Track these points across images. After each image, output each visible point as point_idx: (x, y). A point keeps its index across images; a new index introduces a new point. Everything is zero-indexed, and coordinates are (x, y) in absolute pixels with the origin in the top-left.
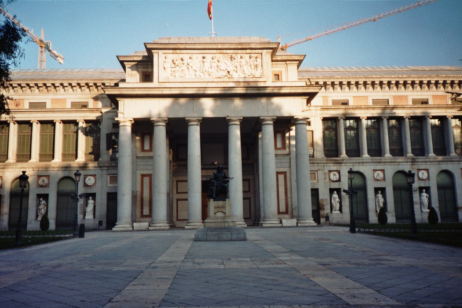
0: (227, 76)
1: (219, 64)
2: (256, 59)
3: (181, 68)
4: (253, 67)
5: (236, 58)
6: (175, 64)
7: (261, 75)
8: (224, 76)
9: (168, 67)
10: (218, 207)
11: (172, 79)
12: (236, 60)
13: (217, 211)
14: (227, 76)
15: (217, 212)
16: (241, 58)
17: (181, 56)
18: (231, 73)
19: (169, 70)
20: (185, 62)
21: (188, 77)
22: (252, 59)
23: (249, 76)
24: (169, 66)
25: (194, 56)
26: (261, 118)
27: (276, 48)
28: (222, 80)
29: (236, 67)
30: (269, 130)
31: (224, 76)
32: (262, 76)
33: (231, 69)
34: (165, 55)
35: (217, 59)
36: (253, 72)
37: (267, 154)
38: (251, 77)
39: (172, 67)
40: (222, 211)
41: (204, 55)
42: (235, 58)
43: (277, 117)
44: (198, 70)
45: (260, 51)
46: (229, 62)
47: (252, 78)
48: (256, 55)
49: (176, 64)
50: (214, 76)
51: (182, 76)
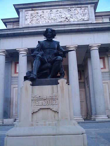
1: (61, 14)
7: (88, 19)
9: (28, 18)
10: (40, 99)
11: (31, 25)
12: (71, 12)
13: (39, 107)
15: (39, 110)
18: (68, 19)
21: (41, 23)
22: (82, 10)
25: (45, 11)
27: (97, 2)
28: (63, 23)
30: (95, 54)
33: (68, 16)
34: (26, 12)
35: (59, 11)
36: (83, 18)
38: (82, 20)
40: (51, 107)
41: (51, 10)
42: (71, 10)
43: (101, 44)
44: (47, 18)
45: (86, 5)
46: (67, 13)
48: (84, 8)
50: (57, 21)
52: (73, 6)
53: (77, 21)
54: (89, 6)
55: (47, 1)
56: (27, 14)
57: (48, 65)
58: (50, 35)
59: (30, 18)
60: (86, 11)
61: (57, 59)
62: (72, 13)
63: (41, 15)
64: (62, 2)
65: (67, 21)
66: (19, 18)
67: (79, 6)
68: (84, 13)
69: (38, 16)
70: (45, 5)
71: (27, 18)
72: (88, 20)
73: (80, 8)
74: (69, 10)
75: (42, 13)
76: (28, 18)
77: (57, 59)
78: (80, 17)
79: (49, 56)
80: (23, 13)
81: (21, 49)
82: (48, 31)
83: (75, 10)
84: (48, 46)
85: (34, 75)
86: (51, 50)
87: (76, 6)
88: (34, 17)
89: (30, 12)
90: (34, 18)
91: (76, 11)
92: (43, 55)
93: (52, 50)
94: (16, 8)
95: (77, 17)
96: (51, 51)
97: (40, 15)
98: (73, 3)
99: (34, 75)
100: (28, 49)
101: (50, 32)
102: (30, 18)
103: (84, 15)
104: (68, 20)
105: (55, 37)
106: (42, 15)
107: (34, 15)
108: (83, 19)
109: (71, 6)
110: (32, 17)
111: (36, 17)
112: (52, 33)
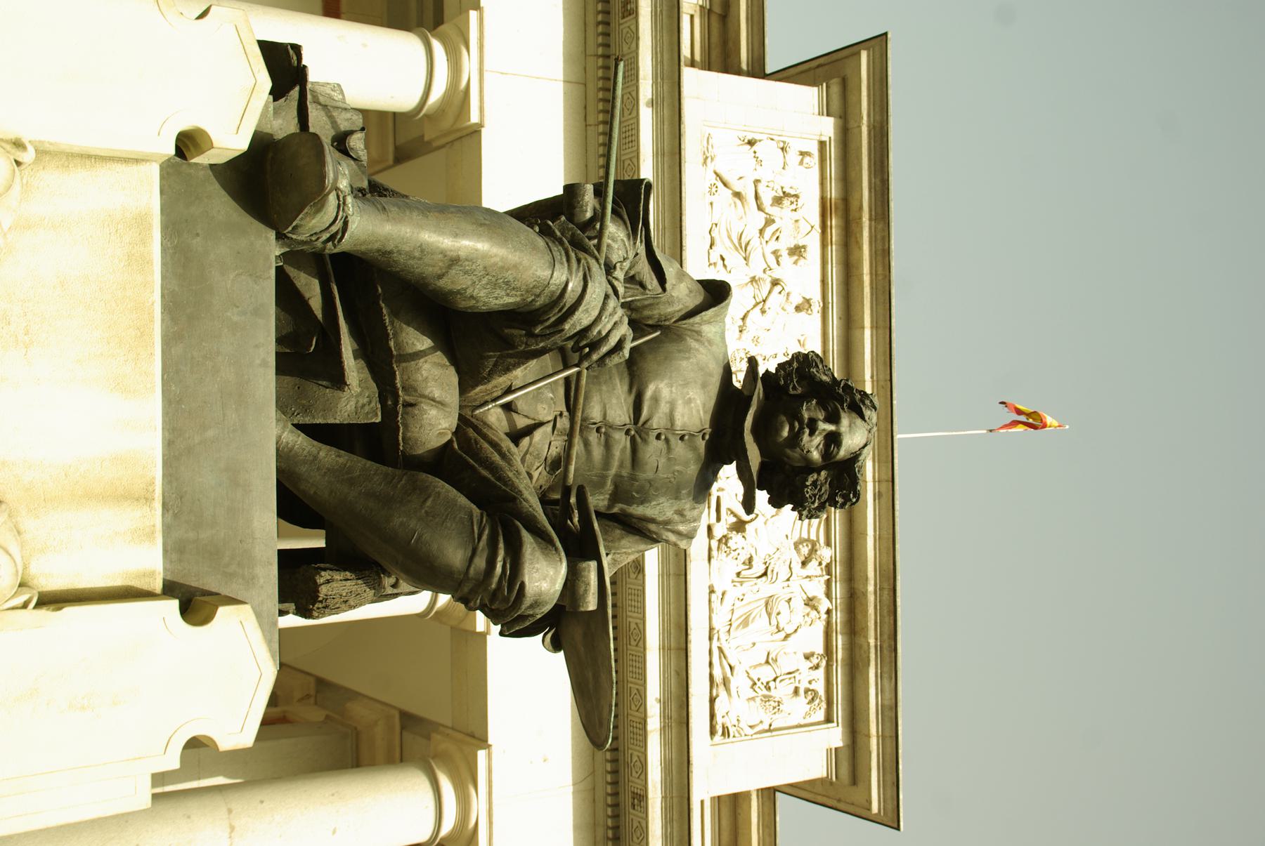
0: (718, 519)
2: (802, 692)
3: (755, 242)
4: (766, 674)
5: (813, 567)
6: (778, 201)
7: (726, 732)
8: (718, 498)
14: (718, 519)
16: (810, 602)
17: (813, 243)
18: (736, 539)
19: (738, 165)
20: (787, 270)
23: (720, 649)
24: (764, 174)
26: (482, 754)
27: (869, 809)
29: (765, 574)
31: (718, 498)
32: (718, 738)
34: (814, 149)
36: (739, 682)
37: (232, 828)
39: (761, 188)
42: (814, 563)
45: (839, 711)
47: (711, 676)
48: (820, 687)
49: (774, 211)
51: (717, 241)
52: (838, 590)
53: (715, 624)
54: (835, 736)
55: (894, 345)
56: (793, 157)
57: (440, 404)
58: (795, 438)
59: (757, 182)
60: (797, 709)
61: (527, 537)
62: (784, 574)
63: (775, 283)
64: (886, 487)
65: (720, 530)
66: (765, 76)
67: (839, 641)
68: (782, 691)
69: (772, 260)
70: (867, 333)
71: (766, 149)
72: (713, 732)
73: (820, 649)
74: (805, 550)
75: (796, 300)
76: (759, 162)
77: (527, 537)
78: (745, 650)
79: (541, 424)
80: (802, 115)
81: (469, 65)
82: (845, 421)
83: (810, 602)
84: (671, 418)
85: (341, 205)
86: (621, 442)
87: (838, 618)
88: (769, 222)
89: (808, 185)
90: (760, 219)
91: (798, 619)
92: (595, 345)
93: (617, 453)
94: (859, 54)
95: (745, 623)
96: (608, 446)
97: (777, 273)
98: (871, 588)
99: (341, 205)
100: (475, 132)
101: (833, 439)
102: (757, 182)
103: (764, 692)
104: (724, 540)
105: (762, 496)
106: (776, 299)
107: (783, 215)
108: (726, 682)
109: (838, 570)
110: (767, 199)
111: (769, 231)
112: (810, 468)
